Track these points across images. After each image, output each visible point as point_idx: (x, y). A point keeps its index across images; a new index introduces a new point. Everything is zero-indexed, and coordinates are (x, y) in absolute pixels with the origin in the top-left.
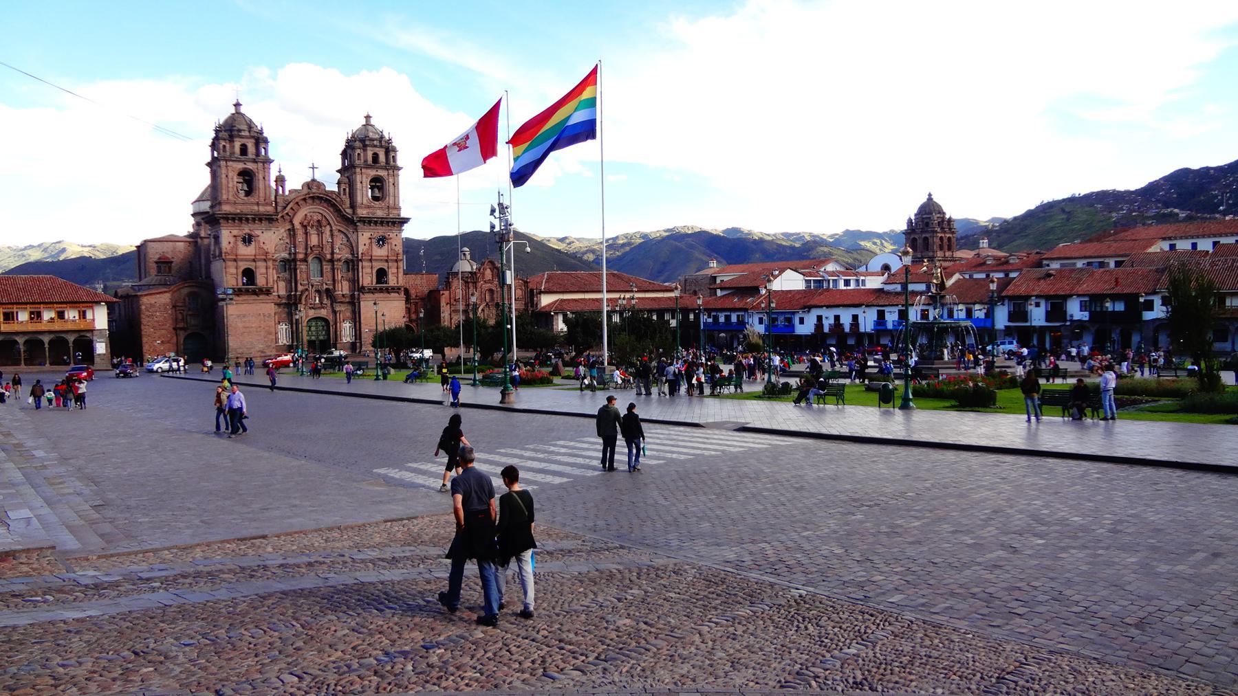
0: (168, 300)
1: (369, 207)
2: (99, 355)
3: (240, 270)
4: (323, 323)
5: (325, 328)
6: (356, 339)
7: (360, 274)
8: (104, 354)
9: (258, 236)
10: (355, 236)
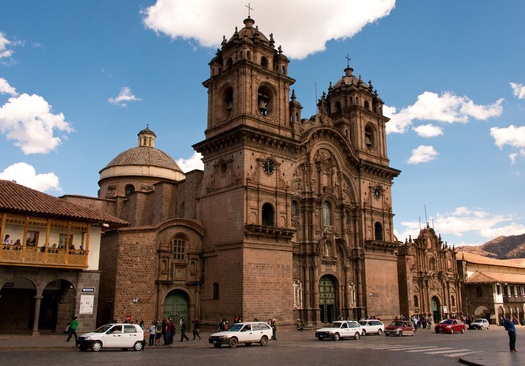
0: (152, 242)
1: (367, 154)
2: (83, 316)
3: (262, 204)
5: (332, 289)
6: (358, 305)
7: (363, 226)
8: (91, 316)
9: (279, 165)
10: (357, 183)
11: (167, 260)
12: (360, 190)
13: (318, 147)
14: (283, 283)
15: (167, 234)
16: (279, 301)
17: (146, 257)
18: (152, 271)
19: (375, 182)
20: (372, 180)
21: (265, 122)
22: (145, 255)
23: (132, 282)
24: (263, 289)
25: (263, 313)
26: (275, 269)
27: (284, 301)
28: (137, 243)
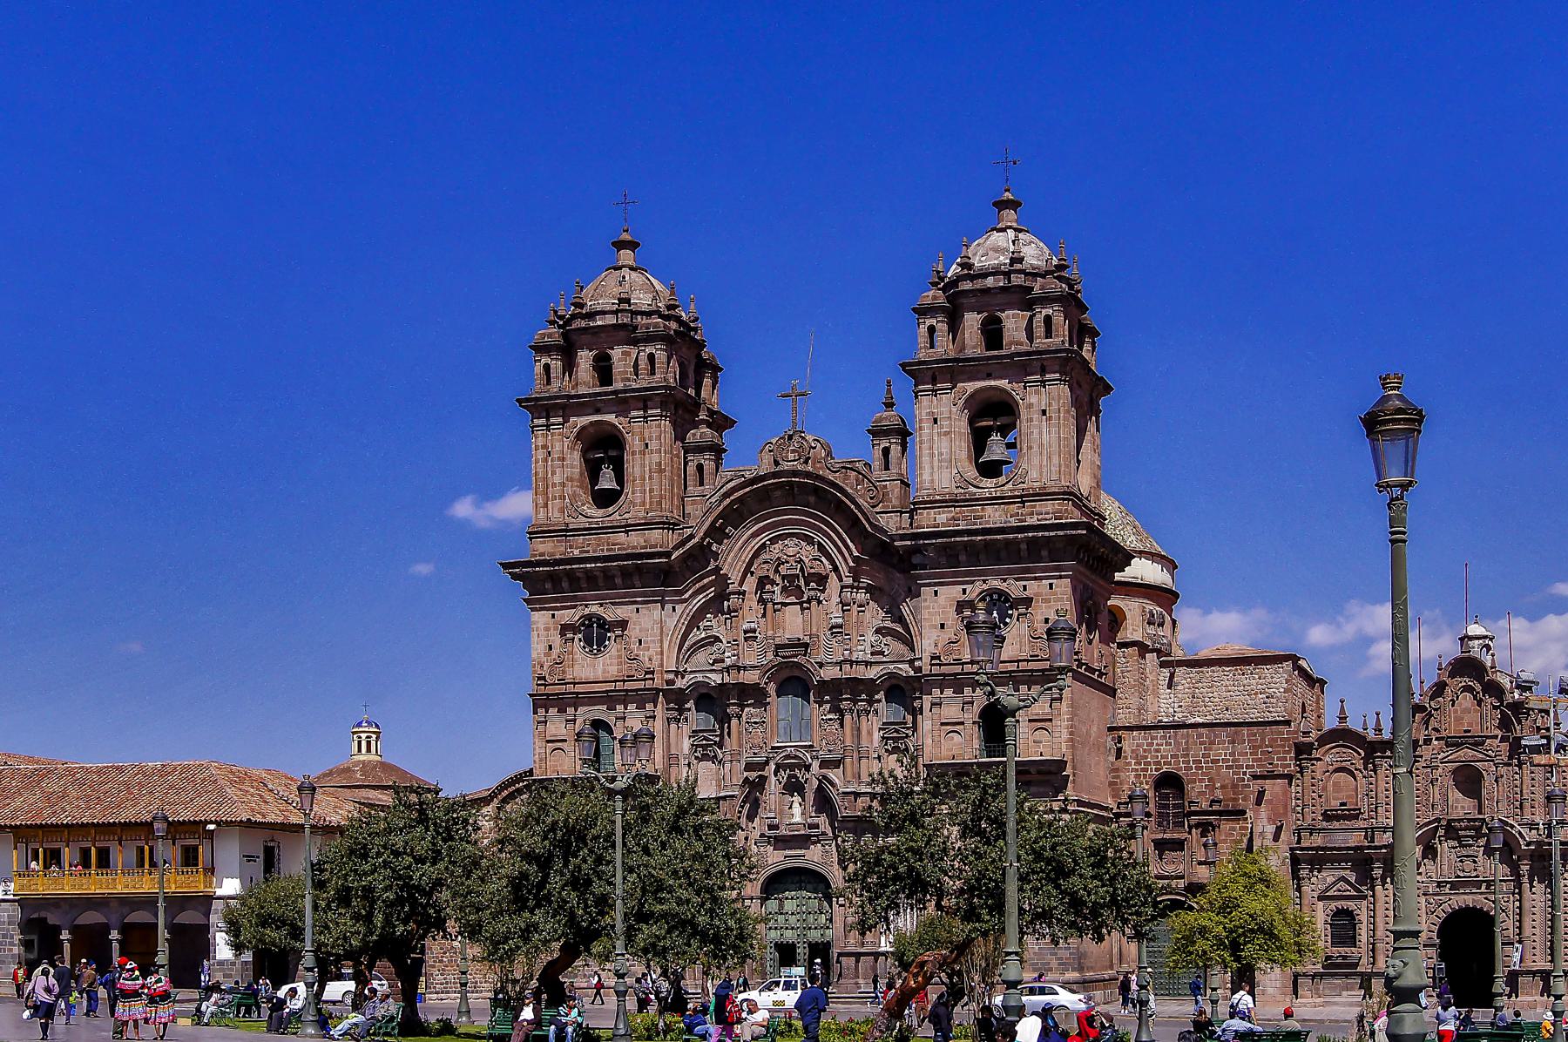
9: (623, 624)
13: (764, 538)
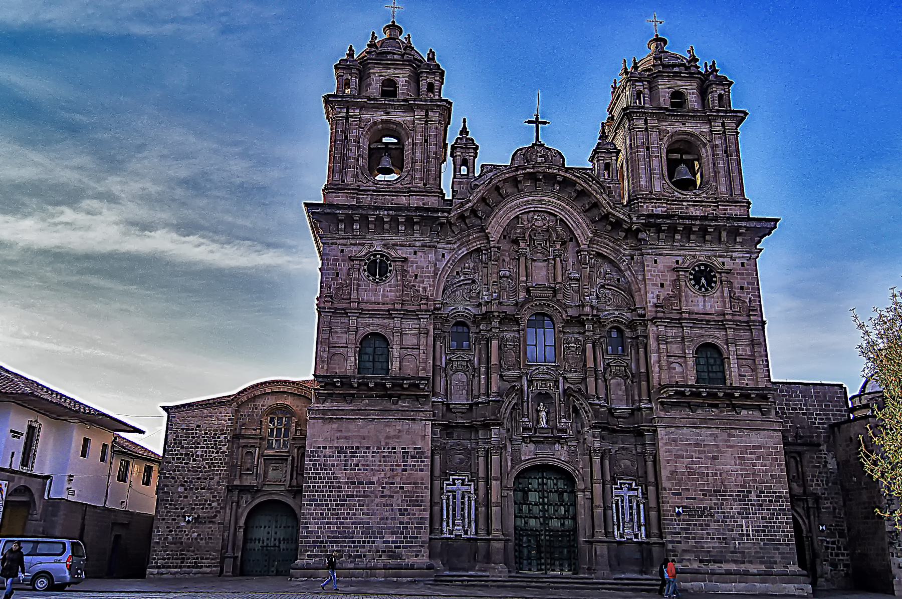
4: (561, 485)
11: (252, 450)
12: (644, 279)
14: (404, 483)
15: (256, 409)
16: (392, 519)
17: (212, 448)
18: (222, 470)
19: (694, 257)
20: (682, 252)
21: (374, 191)
22: (211, 444)
23: (186, 489)
24: (353, 496)
25: (348, 542)
26: (384, 457)
27: (405, 519)
28: (199, 426)
